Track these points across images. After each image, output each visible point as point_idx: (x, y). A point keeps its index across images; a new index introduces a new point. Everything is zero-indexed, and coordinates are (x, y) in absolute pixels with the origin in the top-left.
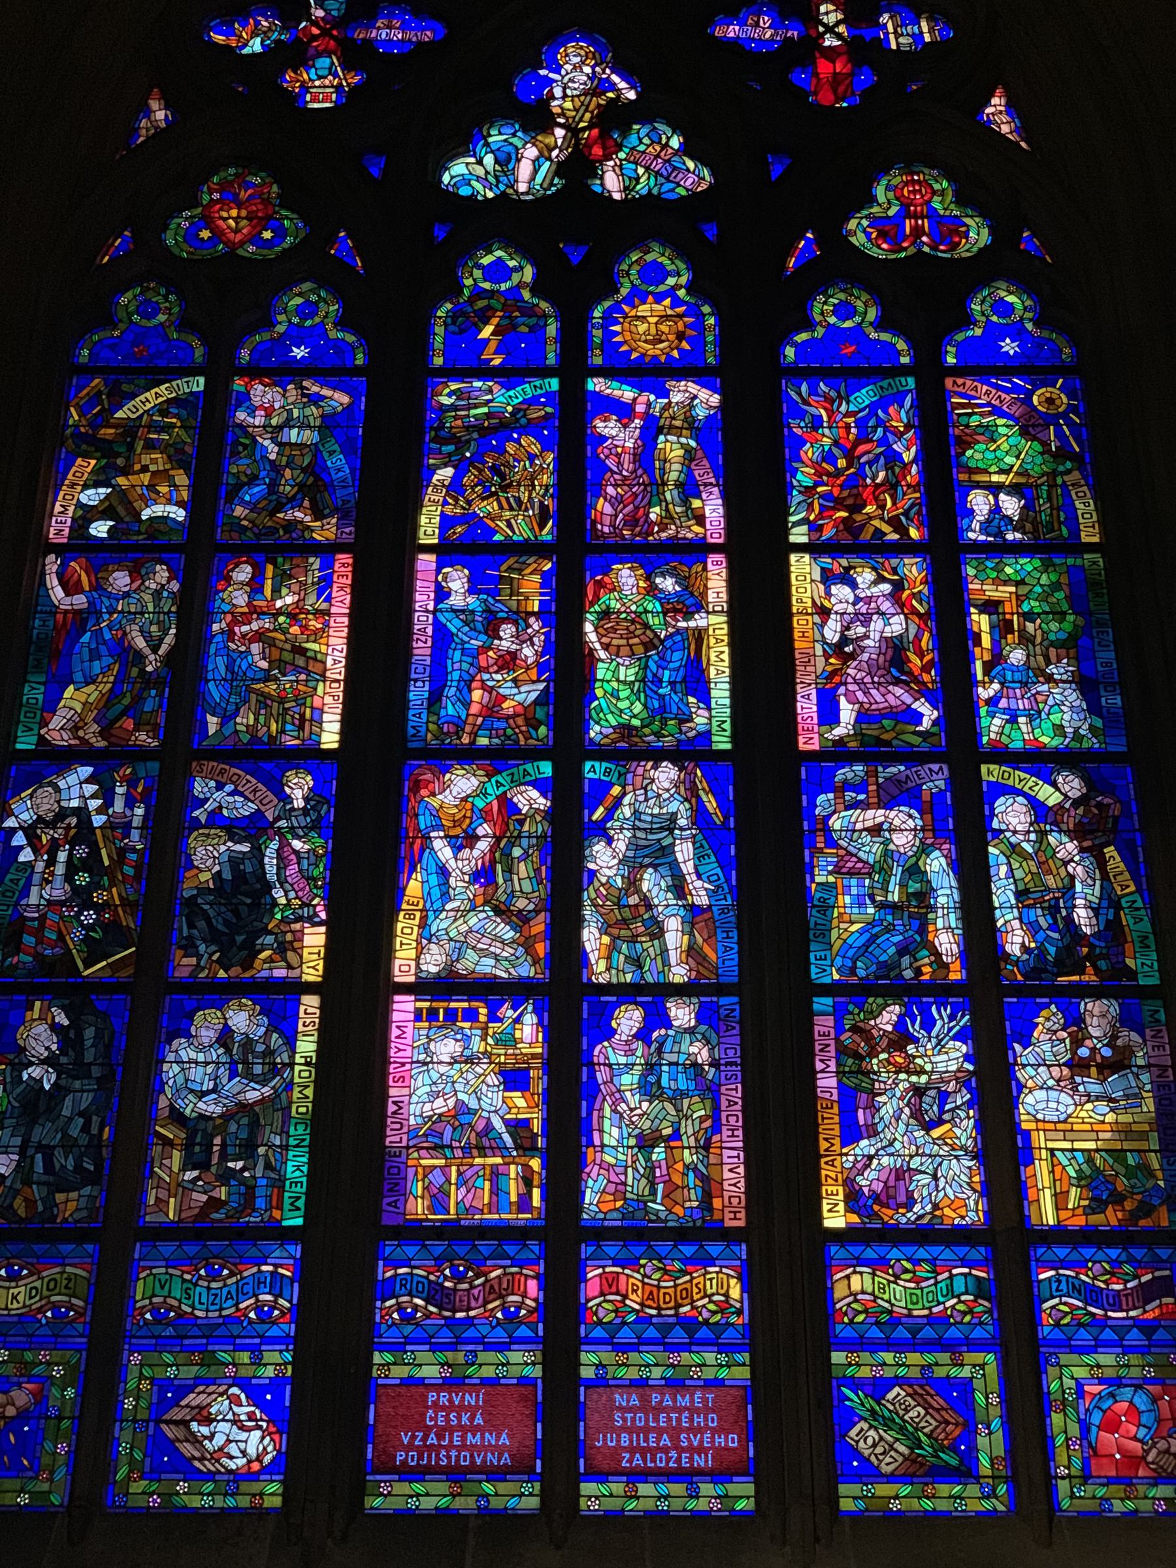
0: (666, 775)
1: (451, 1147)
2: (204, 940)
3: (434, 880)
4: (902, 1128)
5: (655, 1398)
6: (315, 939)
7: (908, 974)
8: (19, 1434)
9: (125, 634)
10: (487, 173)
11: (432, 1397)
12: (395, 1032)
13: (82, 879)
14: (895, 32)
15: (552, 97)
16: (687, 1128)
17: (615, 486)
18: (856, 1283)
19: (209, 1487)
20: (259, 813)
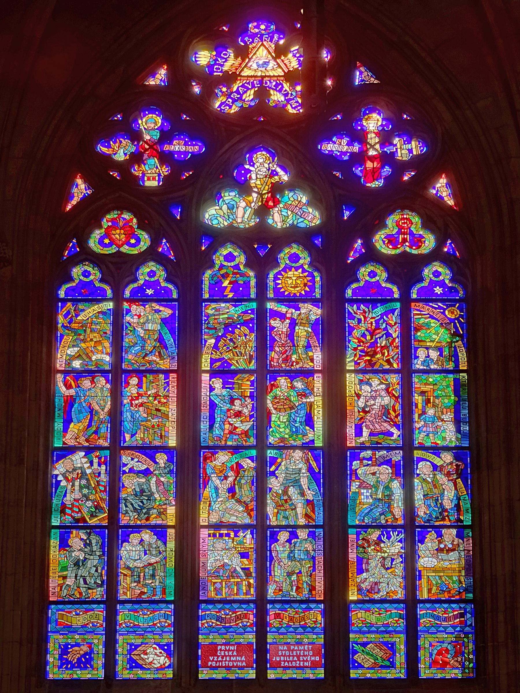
3: (213, 491)
6: (171, 510)
12: (201, 541)
13: (85, 491)
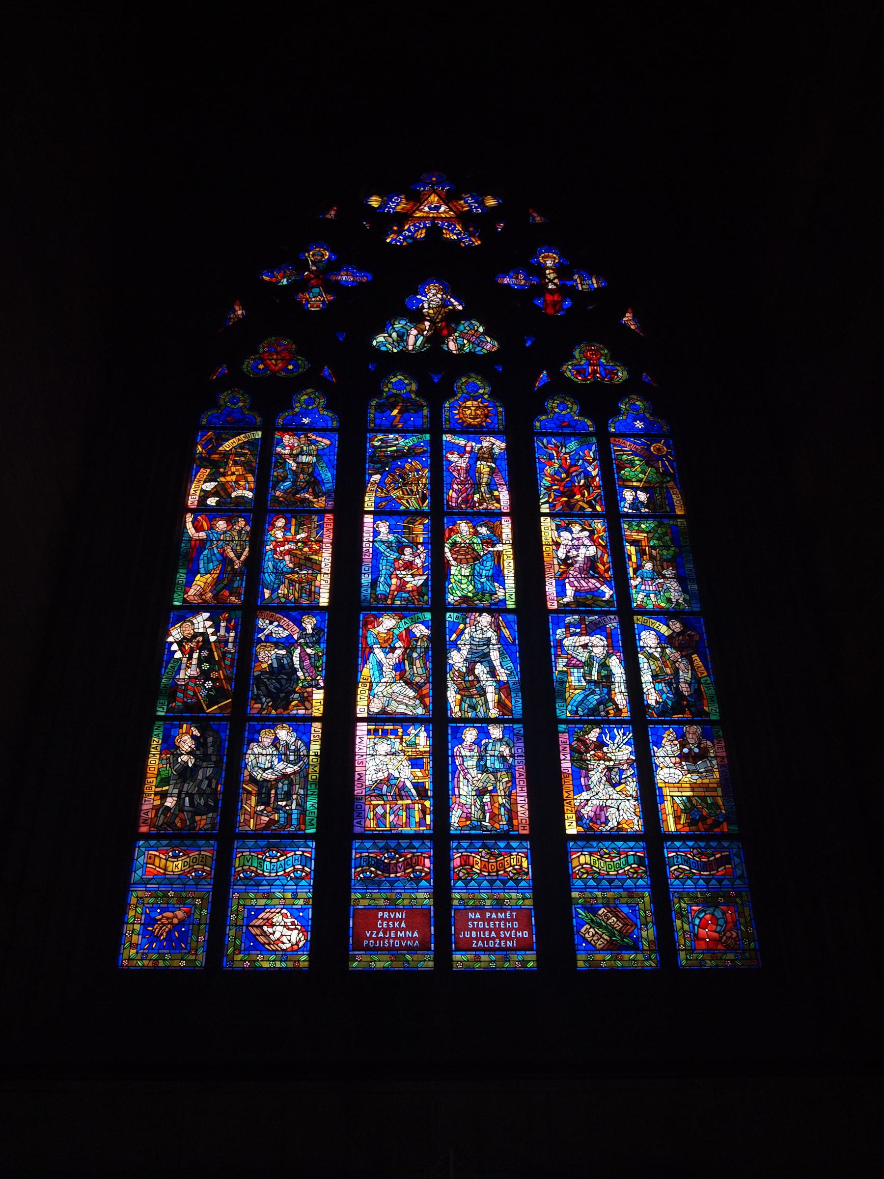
0: (485, 619)
4: (602, 786)
5: (488, 914)
6: (318, 696)
8: (180, 931)
9: (224, 551)
11: (380, 914)
12: (358, 740)
13: (206, 666)
16: (501, 787)
17: (457, 484)
19: (273, 957)
20: (290, 636)
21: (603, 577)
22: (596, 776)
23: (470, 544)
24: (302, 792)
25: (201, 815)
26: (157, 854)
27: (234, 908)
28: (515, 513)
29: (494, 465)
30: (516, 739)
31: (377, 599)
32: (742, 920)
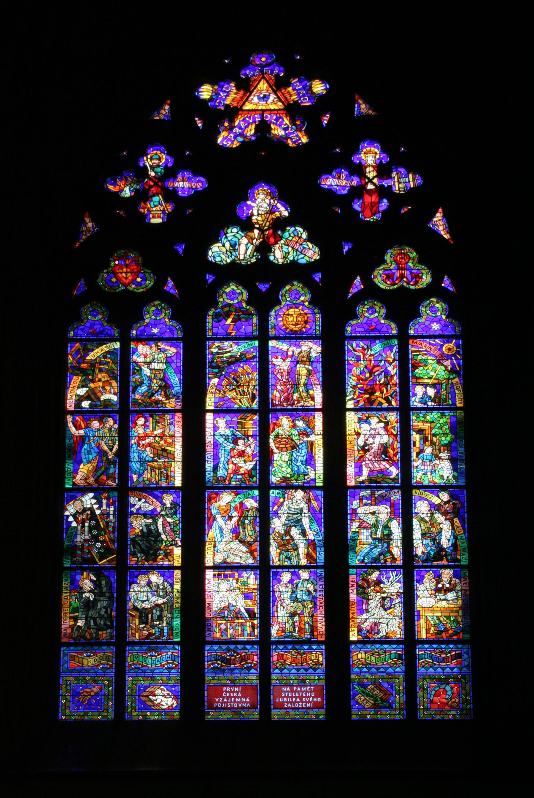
0: (300, 494)
1: (227, 617)
2: (139, 552)
3: (218, 531)
4: (377, 610)
6: (177, 552)
7: (382, 561)
8: (96, 699)
9: (99, 444)
10: (227, 251)
11: (225, 689)
12: (207, 582)
13: (95, 532)
14: (398, 181)
15: (252, 215)
16: (306, 611)
17: (281, 385)
18: (360, 656)
20: (154, 510)
21: (391, 460)
22: (374, 603)
23: (289, 436)
24: (169, 615)
25: (103, 630)
26: (76, 655)
27: (130, 686)
28: (326, 410)
29: (310, 368)
30: (318, 579)
31: (217, 480)
32: (464, 692)
